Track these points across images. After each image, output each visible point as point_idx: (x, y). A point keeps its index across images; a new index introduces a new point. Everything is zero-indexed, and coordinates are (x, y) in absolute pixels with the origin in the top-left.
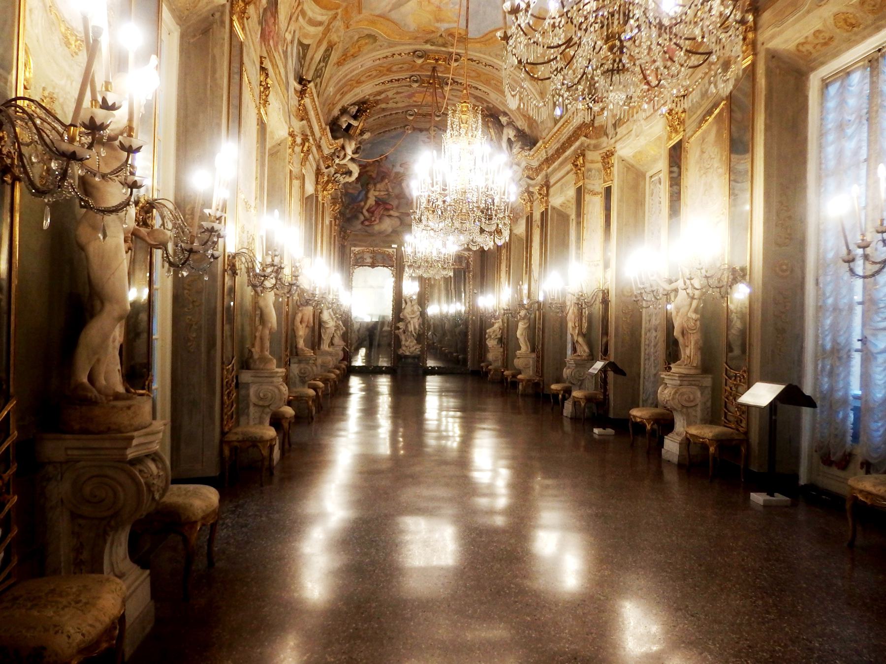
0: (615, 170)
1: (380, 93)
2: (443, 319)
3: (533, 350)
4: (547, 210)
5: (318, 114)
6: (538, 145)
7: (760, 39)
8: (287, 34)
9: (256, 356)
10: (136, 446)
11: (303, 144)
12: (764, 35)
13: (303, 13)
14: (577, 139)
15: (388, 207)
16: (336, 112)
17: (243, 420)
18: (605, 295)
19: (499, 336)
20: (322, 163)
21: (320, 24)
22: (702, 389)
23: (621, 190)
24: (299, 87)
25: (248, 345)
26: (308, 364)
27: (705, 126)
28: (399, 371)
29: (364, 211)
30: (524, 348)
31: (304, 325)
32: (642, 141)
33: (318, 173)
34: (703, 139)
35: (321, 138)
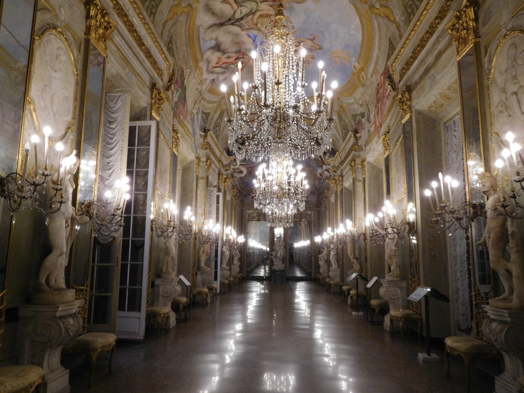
0: (366, 168)
2: (303, 249)
3: (339, 267)
4: (342, 189)
5: (217, 145)
6: (336, 155)
7: (413, 105)
8: (193, 110)
9: (164, 271)
10: (61, 311)
11: (207, 161)
12: (414, 102)
13: (204, 99)
14: (350, 153)
17: (156, 303)
18: (365, 235)
19: (326, 259)
20: (222, 169)
21: (215, 102)
22: (401, 288)
23: (370, 179)
24: (203, 134)
25: (161, 266)
26: (206, 275)
27: (397, 147)
28: (272, 279)
30: (334, 266)
31: (205, 254)
32: (376, 154)
33: (220, 174)
34: (396, 154)
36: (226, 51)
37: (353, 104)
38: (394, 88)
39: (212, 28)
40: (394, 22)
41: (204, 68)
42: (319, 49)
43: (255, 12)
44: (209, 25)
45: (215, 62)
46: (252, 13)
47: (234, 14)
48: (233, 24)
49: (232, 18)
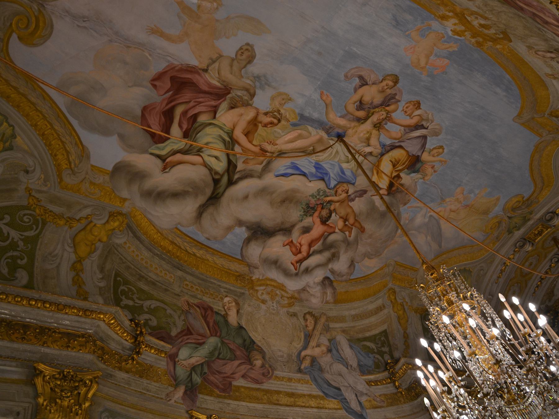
36: (287, 225)
39: (206, 217)
42: (396, 82)
43: (231, 137)
44: (194, 214)
46: (230, 142)
47: (210, 169)
48: (231, 183)
49: (217, 177)
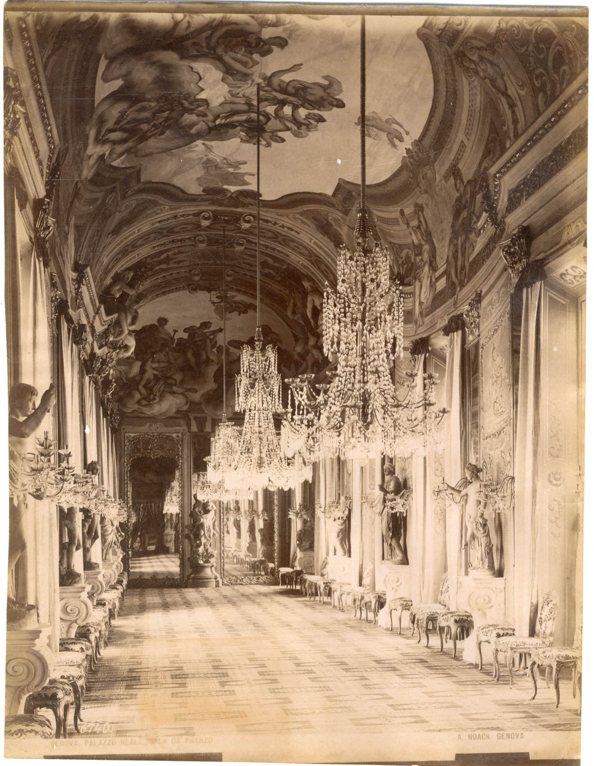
1: (161, 253)
15: (170, 381)
16: (108, 281)
24: (74, 275)
29: (141, 388)
35: (94, 318)
37: (395, 222)
38: (494, 219)
40: (505, 94)
41: (92, 134)
45: (115, 120)
